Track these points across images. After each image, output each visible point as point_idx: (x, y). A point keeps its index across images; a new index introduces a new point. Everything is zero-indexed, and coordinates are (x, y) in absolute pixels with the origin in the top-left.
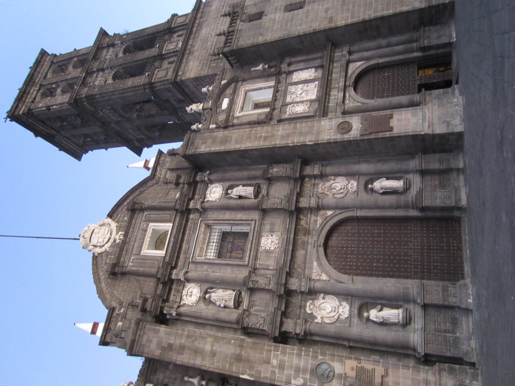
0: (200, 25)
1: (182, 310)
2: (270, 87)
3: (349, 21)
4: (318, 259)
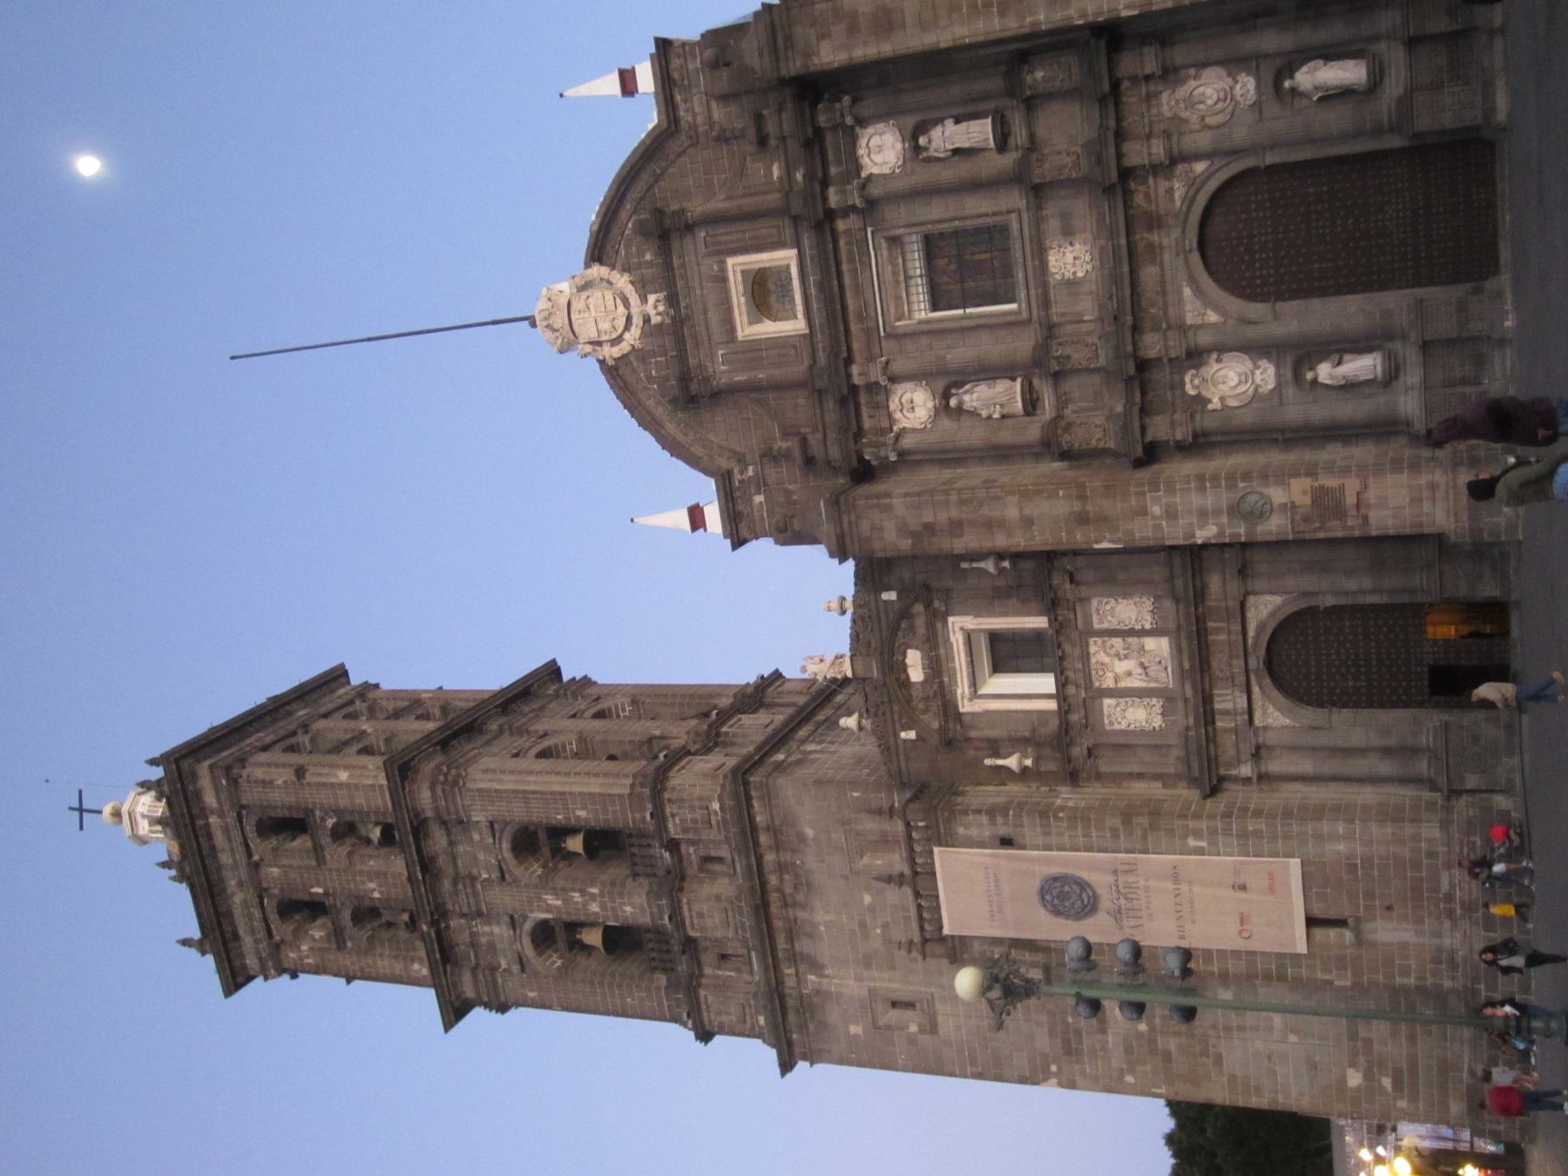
1: (907, 442)
4: (1193, 281)
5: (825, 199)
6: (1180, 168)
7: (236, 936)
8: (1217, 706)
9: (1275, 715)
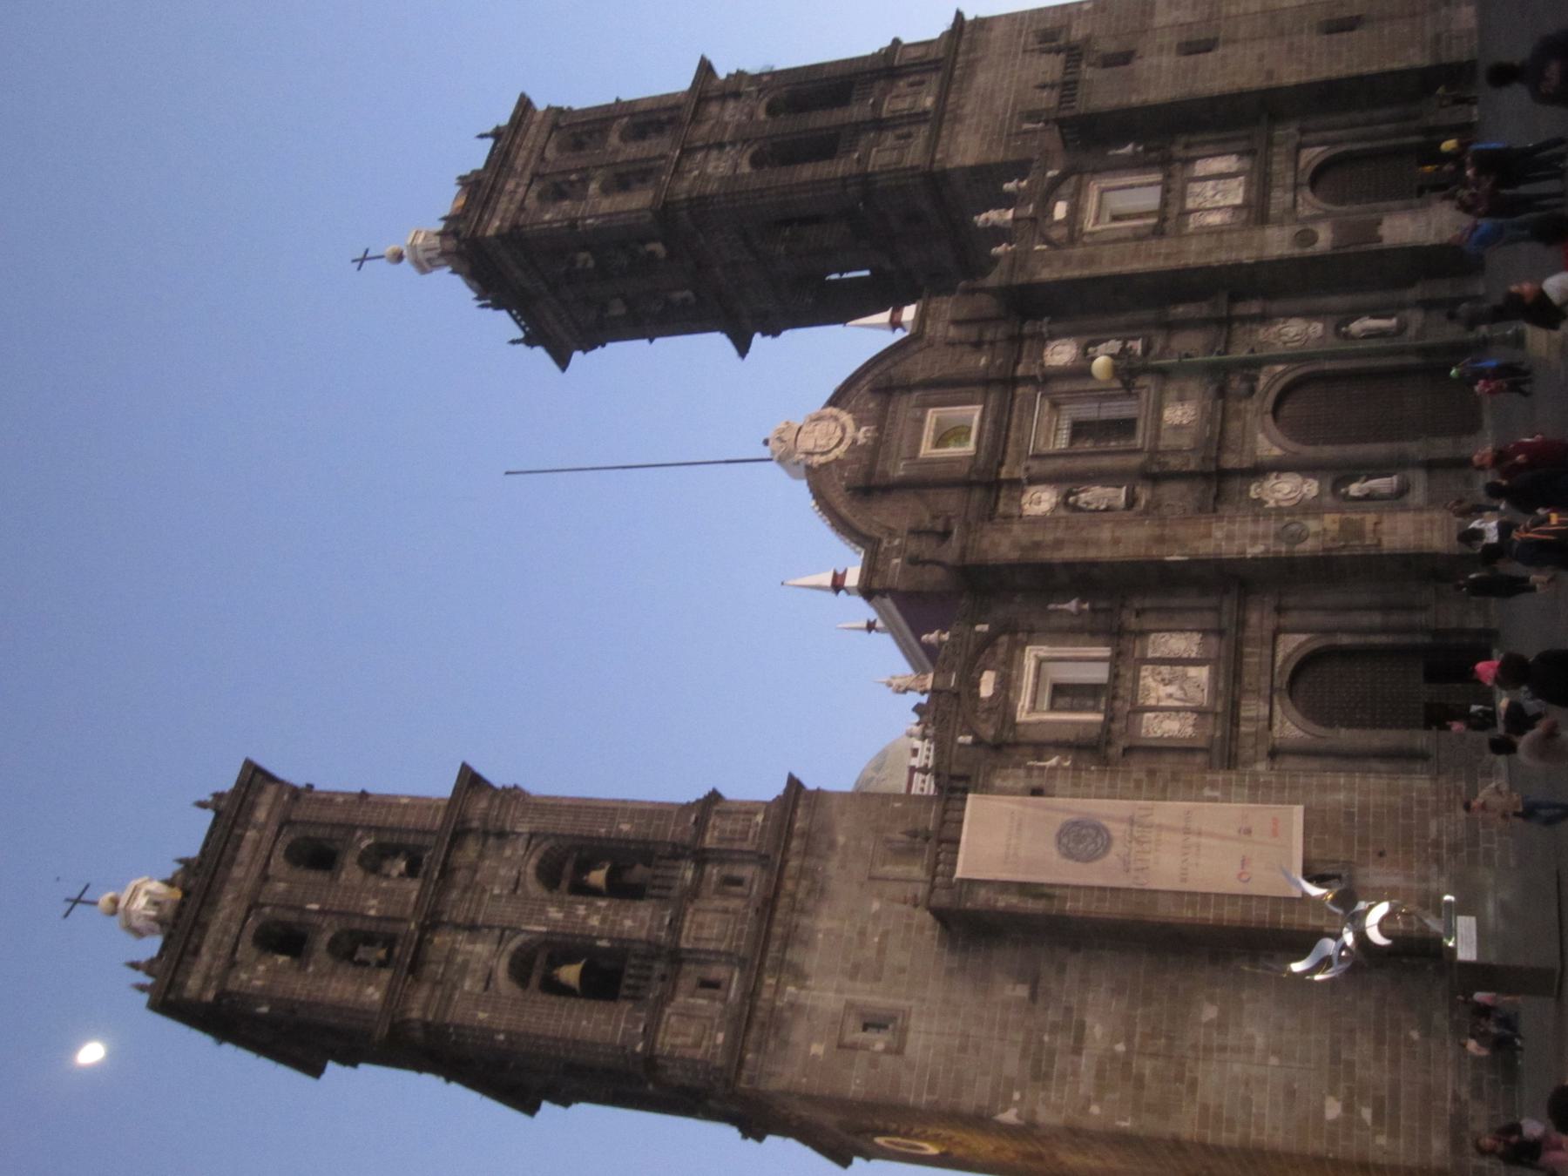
0: (971, 66)
2: (1150, 185)
3: (1304, 79)
4: (1264, 430)
5: (1014, 370)
6: (1266, 369)
7: (196, 952)
8: (1243, 714)
9: (1290, 728)
